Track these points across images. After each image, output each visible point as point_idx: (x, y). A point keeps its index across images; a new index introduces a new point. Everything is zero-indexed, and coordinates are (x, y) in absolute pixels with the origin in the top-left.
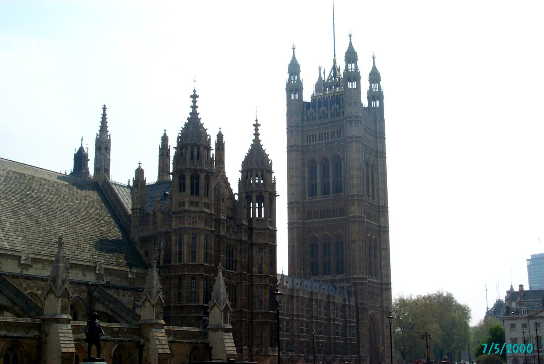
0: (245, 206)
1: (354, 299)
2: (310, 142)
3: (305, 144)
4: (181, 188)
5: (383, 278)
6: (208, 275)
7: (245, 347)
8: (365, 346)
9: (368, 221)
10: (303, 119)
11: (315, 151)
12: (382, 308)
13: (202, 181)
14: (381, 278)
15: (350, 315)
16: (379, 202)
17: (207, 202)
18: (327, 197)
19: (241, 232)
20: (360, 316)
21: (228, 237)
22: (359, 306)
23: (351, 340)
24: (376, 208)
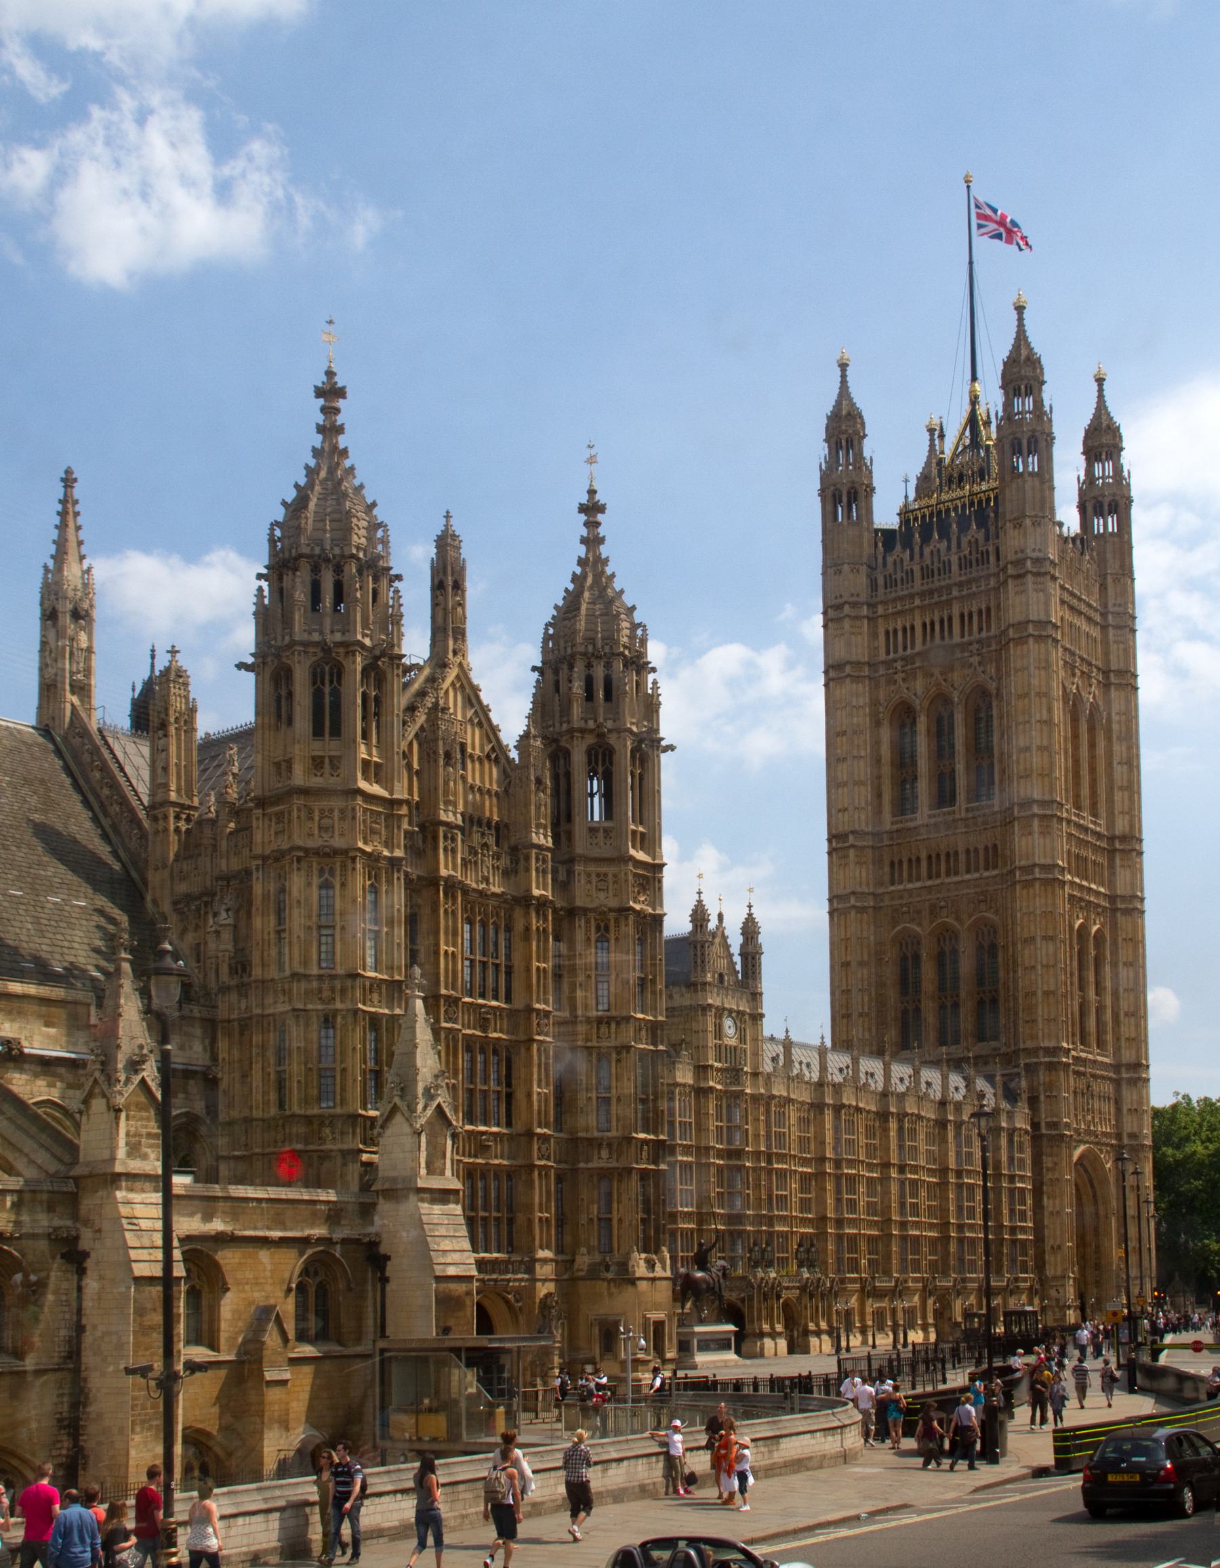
0: (539, 781)
1: (1027, 1111)
2: (896, 651)
3: (882, 656)
4: (279, 716)
5: (1123, 1051)
6: (381, 1011)
7: (543, 1254)
8: (1059, 1247)
9: (1077, 880)
10: (873, 585)
11: (910, 676)
12: (1119, 1136)
13: (355, 689)
14: (1117, 1050)
15: (1011, 1159)
16: (1111, 823)
17: (376, 759)
18: (949, 813)
19: (528, 870)
20: (1047, 1162)
21: (474, 885)
22: (1044, 1131)
23: (1013, 1230)
24: (1104, 844)
